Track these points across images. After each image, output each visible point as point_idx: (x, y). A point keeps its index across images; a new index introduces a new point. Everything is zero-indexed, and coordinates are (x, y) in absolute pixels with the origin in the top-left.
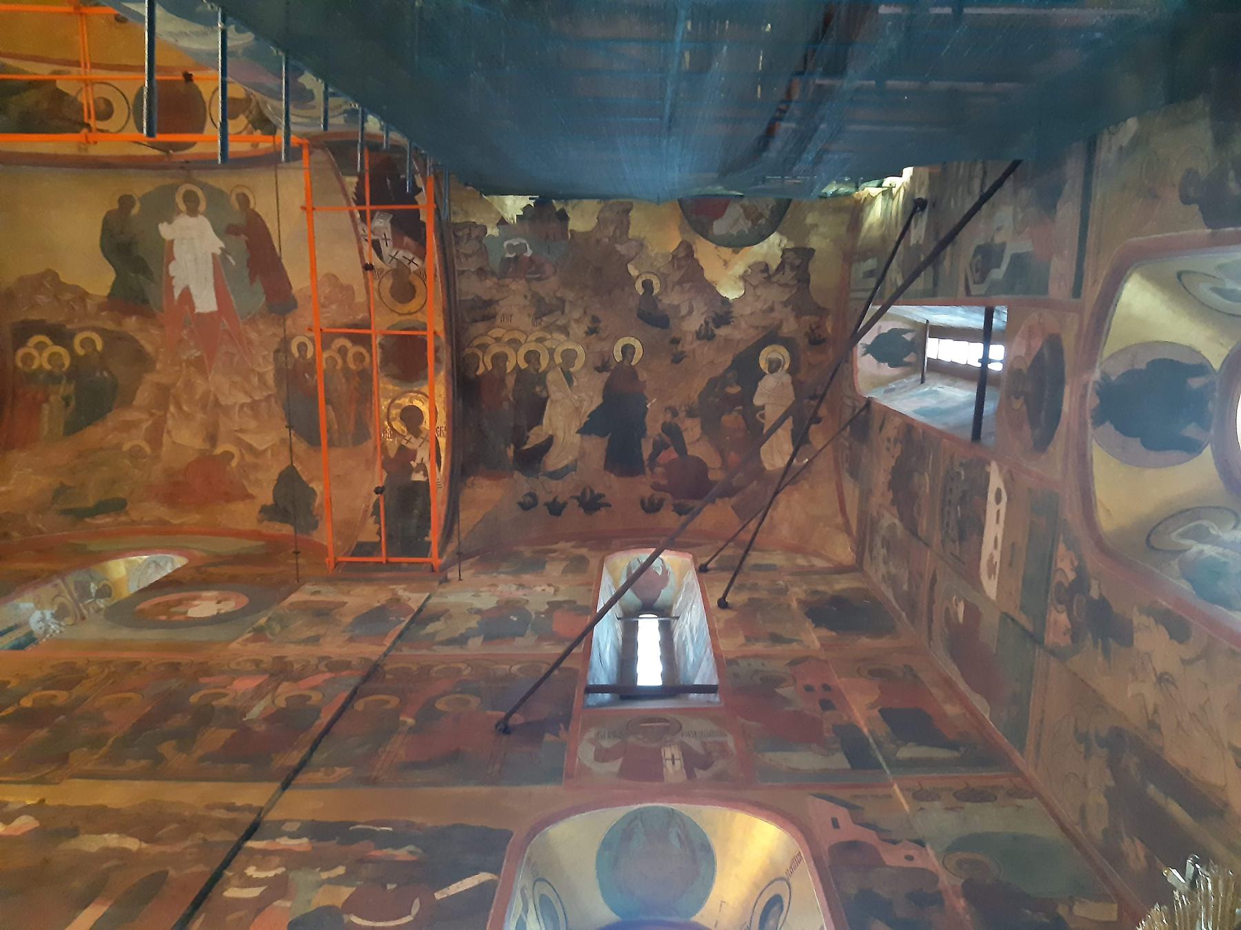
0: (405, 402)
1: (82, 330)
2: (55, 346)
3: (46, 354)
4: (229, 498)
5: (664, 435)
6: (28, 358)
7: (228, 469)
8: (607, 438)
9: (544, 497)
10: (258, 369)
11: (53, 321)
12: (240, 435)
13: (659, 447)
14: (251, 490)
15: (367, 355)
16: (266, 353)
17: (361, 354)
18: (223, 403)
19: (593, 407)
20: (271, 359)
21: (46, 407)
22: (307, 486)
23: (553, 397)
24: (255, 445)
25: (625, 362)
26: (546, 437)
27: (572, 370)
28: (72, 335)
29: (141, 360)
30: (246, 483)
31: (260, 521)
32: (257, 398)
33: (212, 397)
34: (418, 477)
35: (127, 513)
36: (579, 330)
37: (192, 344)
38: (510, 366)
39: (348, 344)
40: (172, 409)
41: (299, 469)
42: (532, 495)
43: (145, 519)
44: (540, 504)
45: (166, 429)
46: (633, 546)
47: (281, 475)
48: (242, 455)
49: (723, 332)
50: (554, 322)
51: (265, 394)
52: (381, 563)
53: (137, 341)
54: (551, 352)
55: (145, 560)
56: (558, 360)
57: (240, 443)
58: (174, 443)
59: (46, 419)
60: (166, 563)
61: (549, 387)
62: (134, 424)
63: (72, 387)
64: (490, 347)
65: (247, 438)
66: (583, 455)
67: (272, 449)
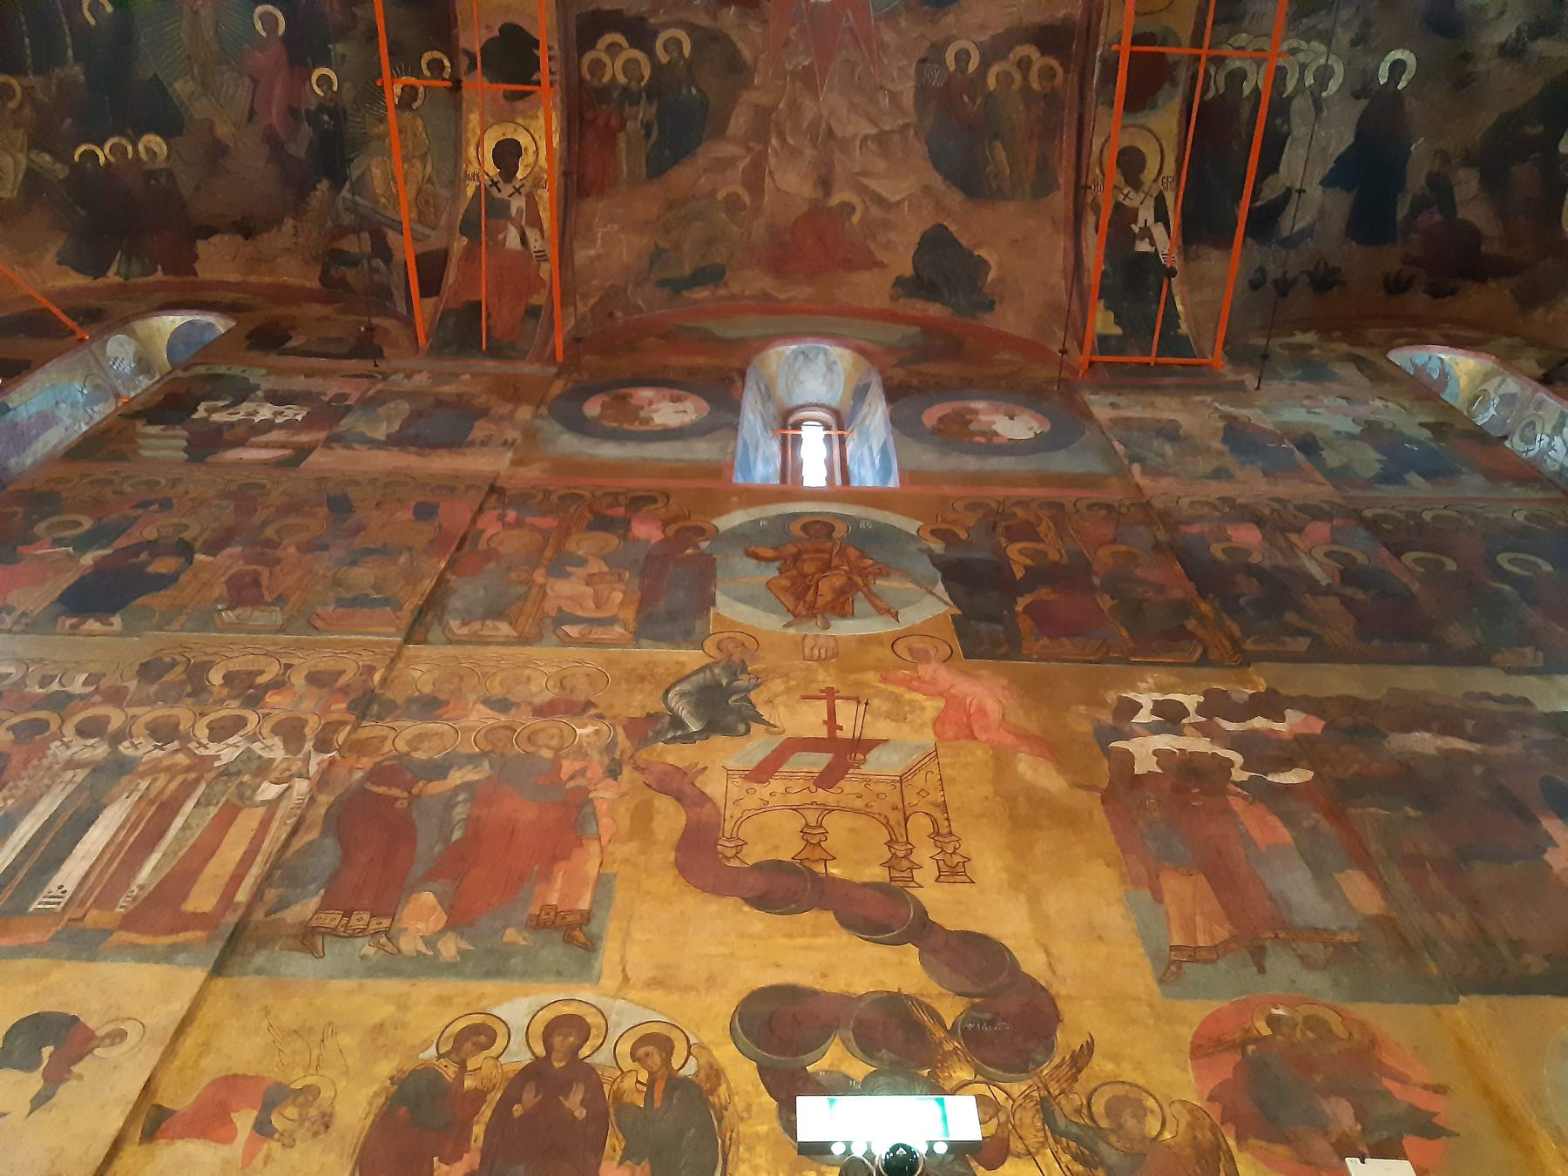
0: (1125, 141)
1: (666, 26)
2: (631, 50)
3: (619, 63)
4: (850, 266)
5: (1428, 190)
6: (597, 66)
7: (847, 224)
8: (1354, 193)
9: (1274, 272)
10: (890, 86)
11: (633, 12)
12: (865, 181)
13: (1419, 207)
14: (882, 256)
15: (1060, 70)
16: (906, 63)
17: (1052, 68)
18: (839, 135)
19: (1343, 149)
20: (912, 72)
21: (621, 136)
22: (971, 254)
23: (1295, 132)
24: (884, 194)
25: (1391, 84)
26: (1284, 190)
27: (1324, 94)
28: (654, 35)
29: (736, 70)
30: (873, 247)
31: (894, 298)
32: (887, 128)
33: (824, 125)
34: (1143, 246)
35: (726, 285)
36: (1344, 37)
37: (801, 47)
38: (1247, 88)
39: (1032, 51)
40: (774, 142)
41: (953, 228)
42: (1262, 270)
43: (747, 293)
44: (1270, 278)
45: (767, 172)
46: (1402, 341)
47: (924, 237)
48: (867, 209)
49: (1542, 46)
50: (1314, 26)
51: (900, 122)
52: (1148, 364)
53: (733, 45)
54: (1303, 67)
55: (793, 351)
56: (1309, 81)
57: (863, 190)
58: (779, 190)
59: (623, 154)
60: (817, 355)
61: (1292, 119)
62: (730, 162)
63: (654, 108)
64: (1227, 61)
65: (873, 184)
66: (1322, 213)
67: (910, 200)
